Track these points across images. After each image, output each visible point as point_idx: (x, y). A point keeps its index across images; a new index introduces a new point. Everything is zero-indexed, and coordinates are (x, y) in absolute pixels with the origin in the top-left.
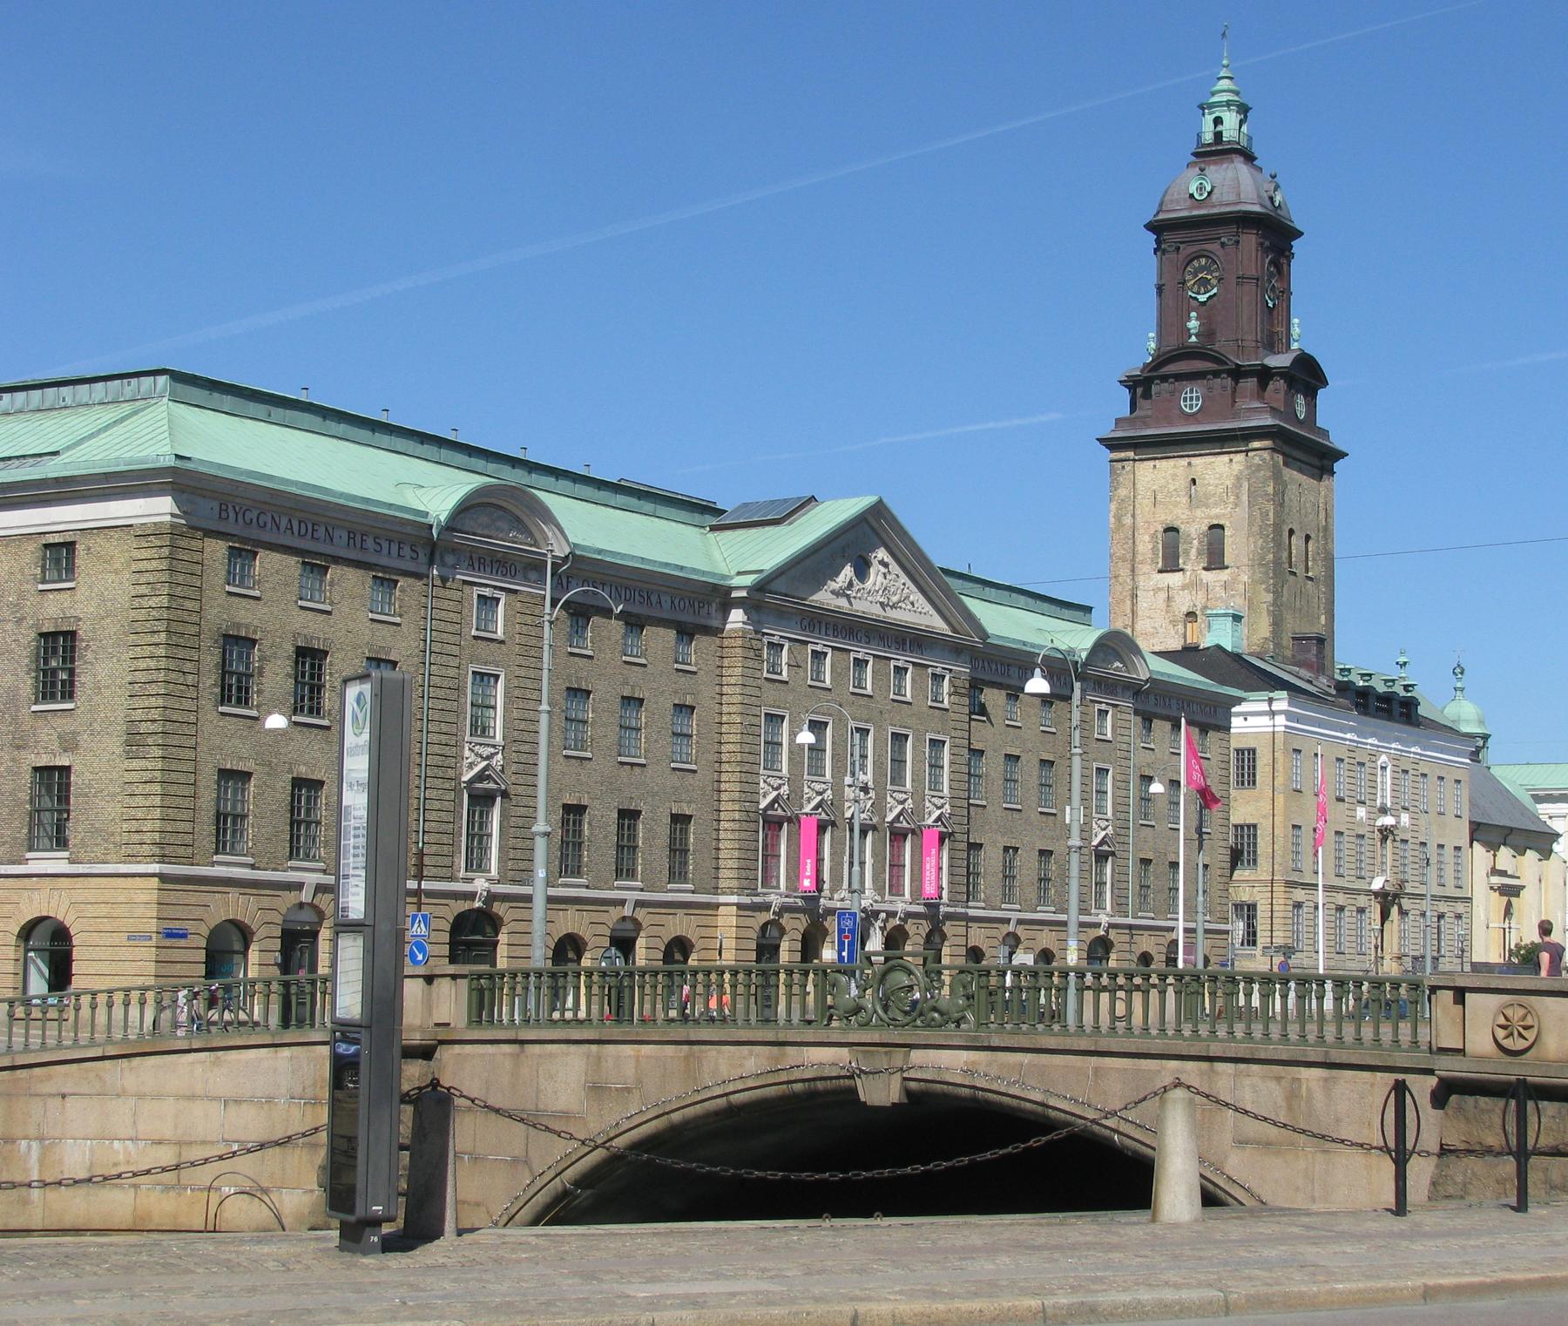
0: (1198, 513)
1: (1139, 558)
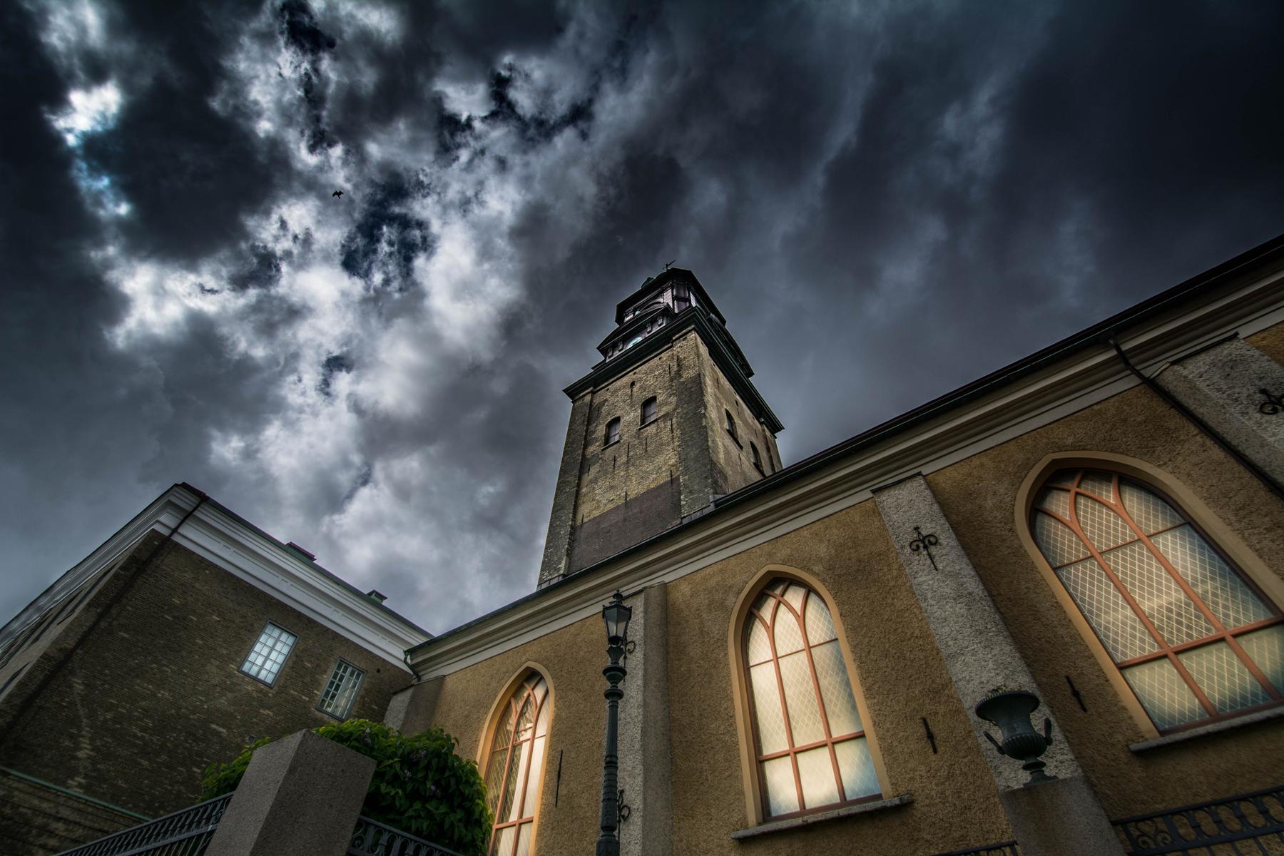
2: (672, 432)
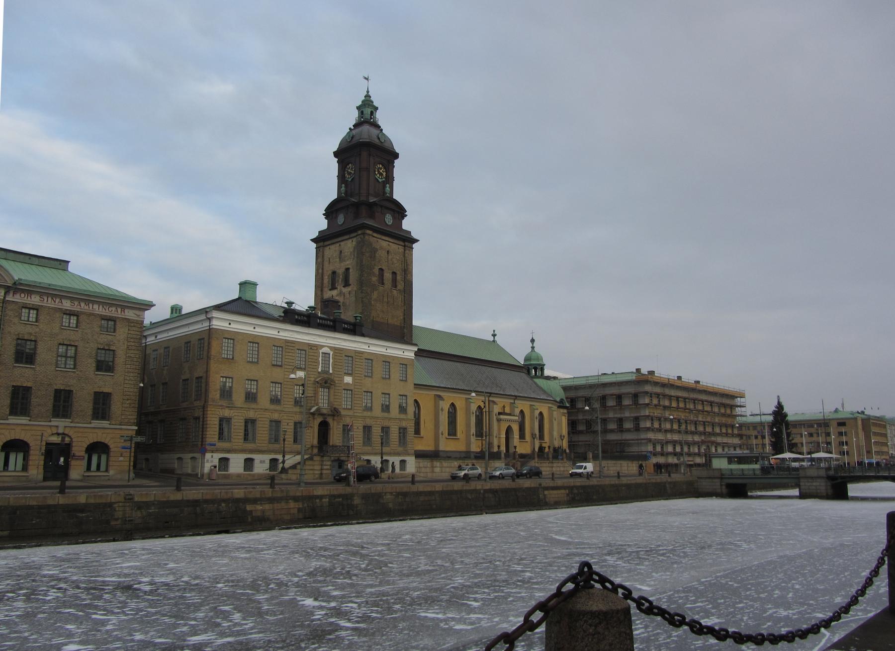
0: (342, 264)
1: (324, 285)
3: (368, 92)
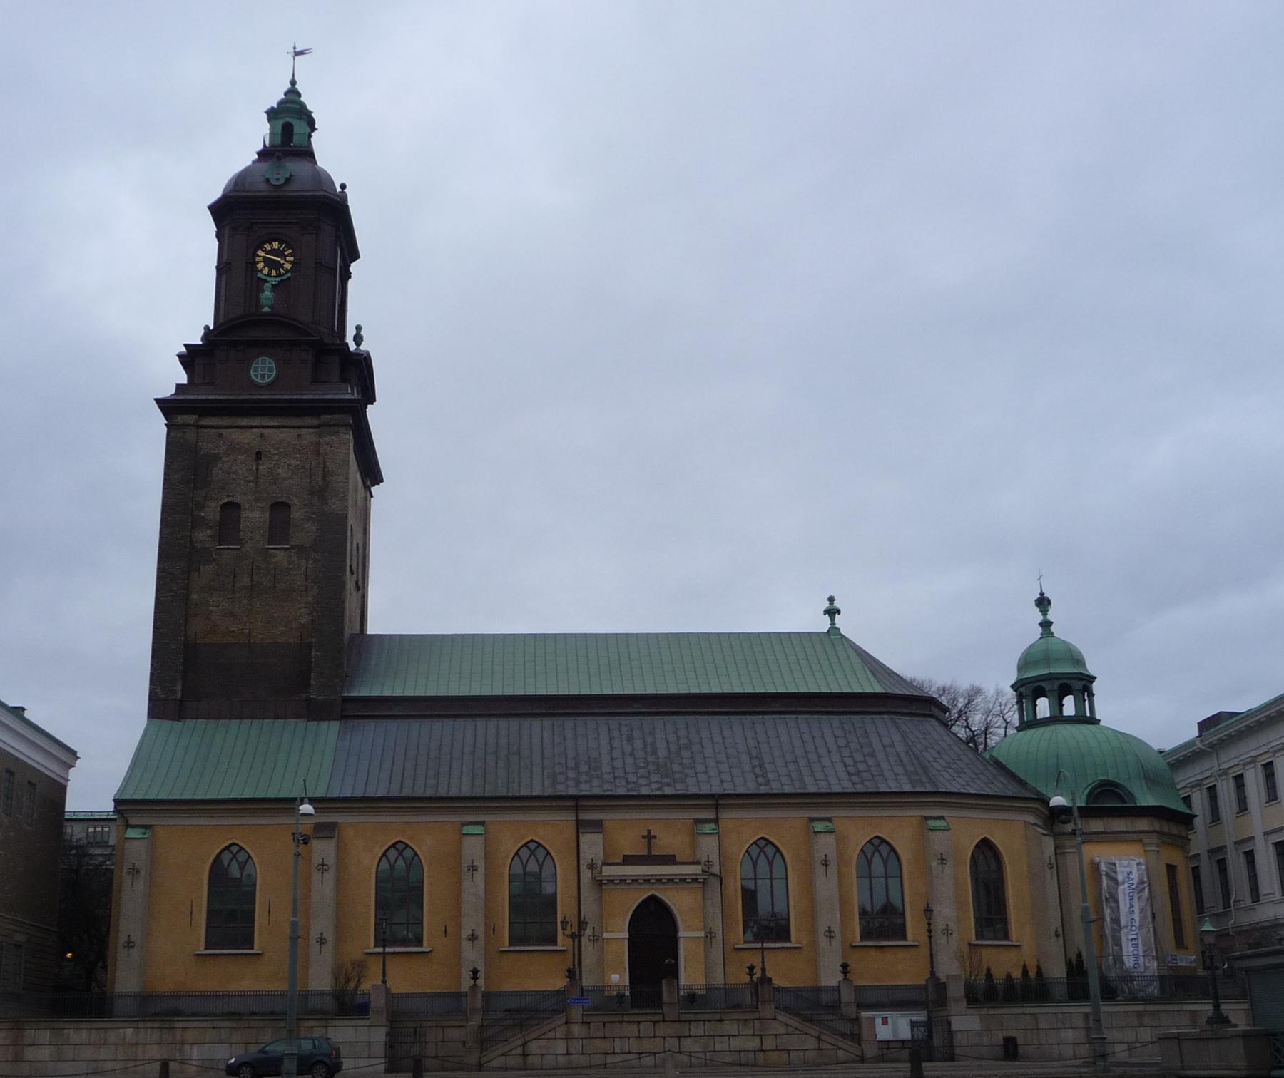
2: (307, 580)
3: (293, 82)
